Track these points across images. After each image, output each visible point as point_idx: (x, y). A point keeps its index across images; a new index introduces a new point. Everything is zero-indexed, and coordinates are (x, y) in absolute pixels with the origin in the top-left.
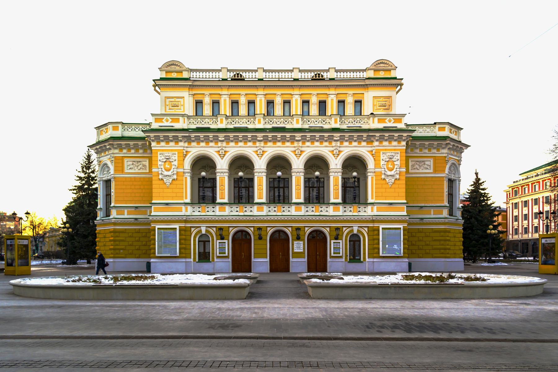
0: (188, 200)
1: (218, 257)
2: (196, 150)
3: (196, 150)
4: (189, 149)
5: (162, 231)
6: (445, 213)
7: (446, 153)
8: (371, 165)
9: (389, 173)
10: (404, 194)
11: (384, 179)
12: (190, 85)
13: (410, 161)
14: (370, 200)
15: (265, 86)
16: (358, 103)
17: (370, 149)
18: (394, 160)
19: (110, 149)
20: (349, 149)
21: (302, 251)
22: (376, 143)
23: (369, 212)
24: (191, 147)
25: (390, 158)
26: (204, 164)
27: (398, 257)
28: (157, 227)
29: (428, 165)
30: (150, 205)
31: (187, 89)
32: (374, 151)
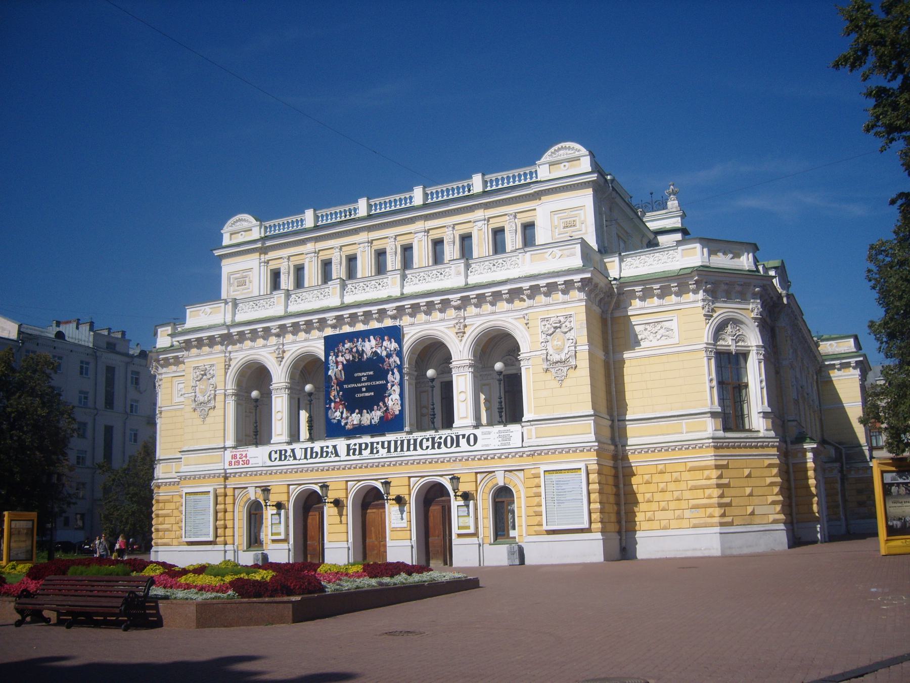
0: (230, 442)
1: (274, 541)
3: (242, 354)
6: (709, 428)
7: (703, 300)
8: (524, 348)
9: (556, 358)
12: (260, 248)
16: (528, 228)
20: (480, 320)
21: (405, 525)
25: (556, 328)
26: (255, 377)
27: (582, 531)
29: (668, 330)
30: (179, 455)
31: (256, 255)
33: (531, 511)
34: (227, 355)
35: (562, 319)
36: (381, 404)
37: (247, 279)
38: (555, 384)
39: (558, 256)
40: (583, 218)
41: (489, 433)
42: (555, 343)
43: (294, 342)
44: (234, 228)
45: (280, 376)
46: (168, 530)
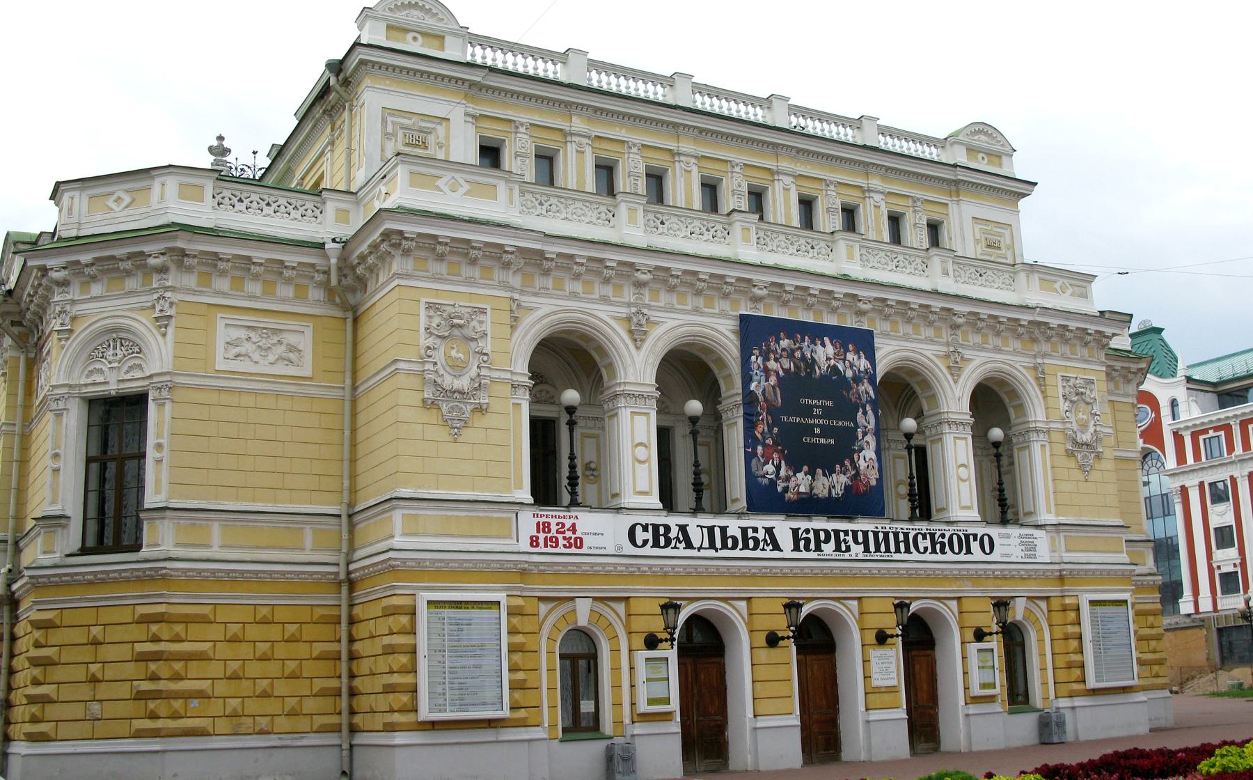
2: (547, 310)
4: (527, 300)
5: (447, 613)
8: (1037, 413)
12: (473, 84)
14: (1046, 516)
15: (701, 131)
19: (163, 270)
23: (1045, 549)
24: (536, 294)
28: (424, 597)
33: (1061, 661)
34: (516, 296)
36: (847, 463)
37: (431, 140)
38: (1079, 475)
40: (1008, 242)
41: (1008, 537)
42: (1080, 415)
43: (671, 309)
44: (400, 16)
45: (637, 368)
46: (201, 695)
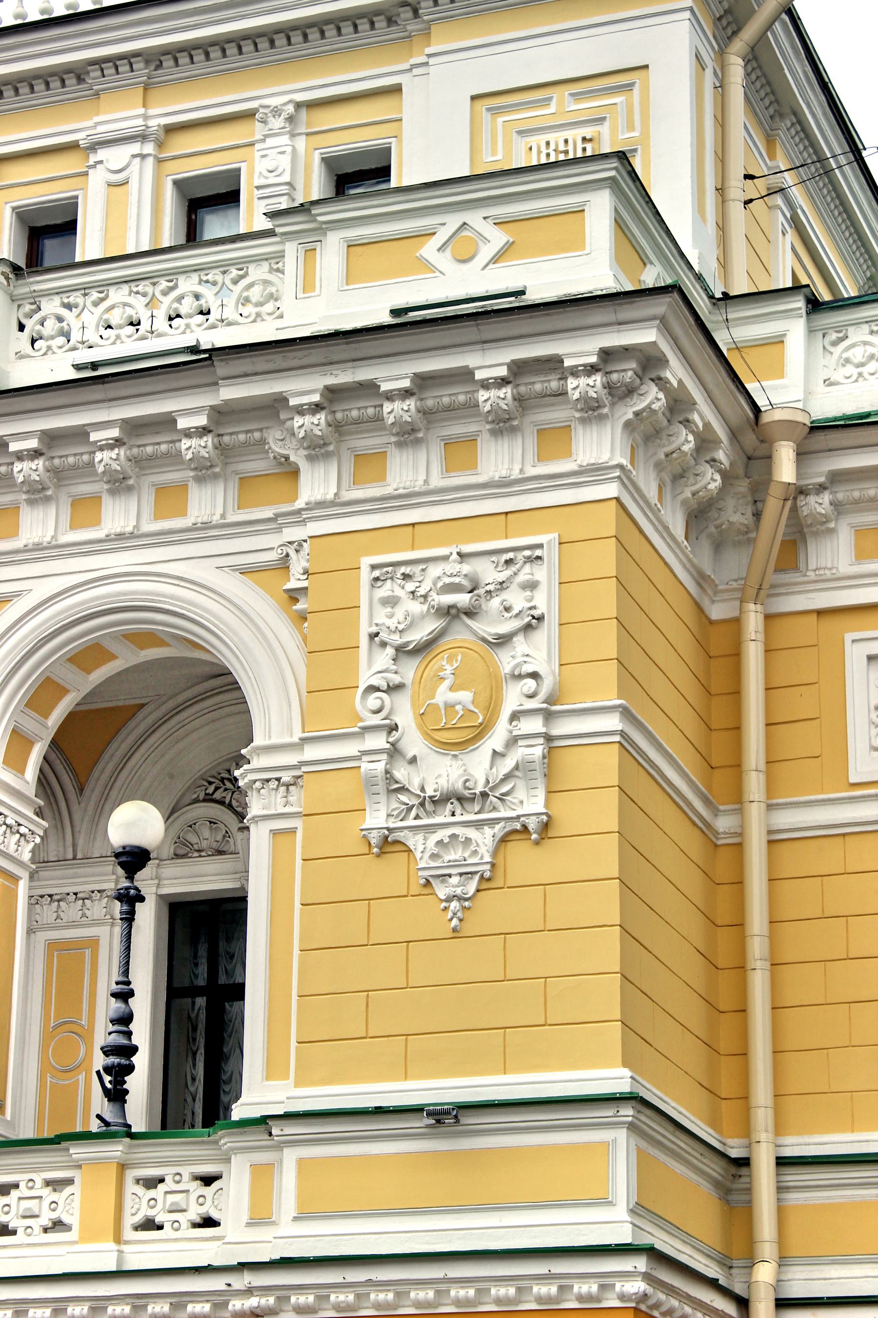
8: (275, 718)
9: (440, 773)
10: (607, 997)
11: (388, 844)
13: (855, 656)
17: (267, 545)
18: (491, 626)
22: (317, 483)
25: (450, 613)
32: (298, 564)
35: (489, 573)
39: (486, 252)
